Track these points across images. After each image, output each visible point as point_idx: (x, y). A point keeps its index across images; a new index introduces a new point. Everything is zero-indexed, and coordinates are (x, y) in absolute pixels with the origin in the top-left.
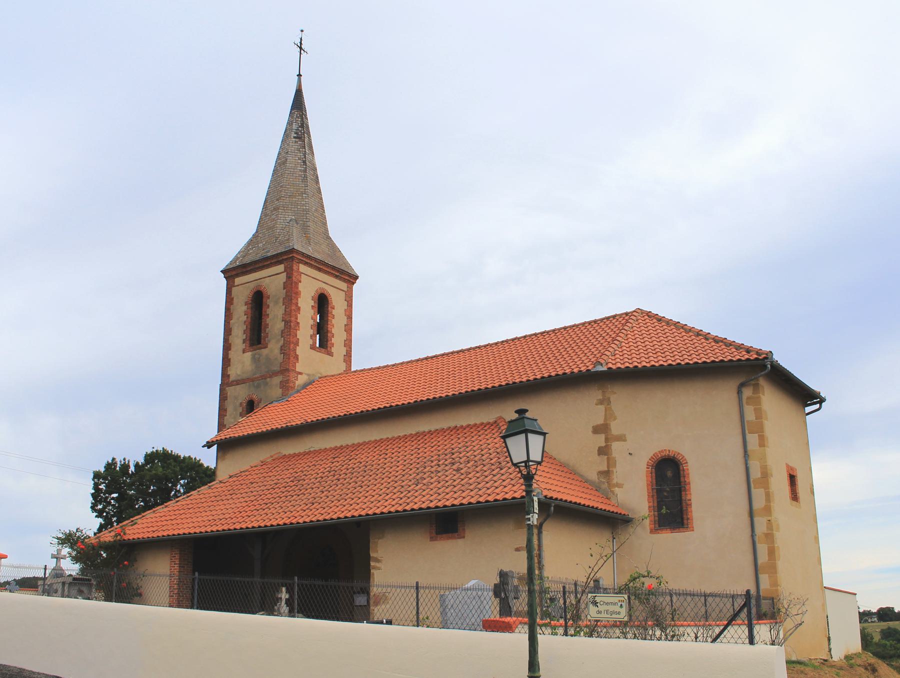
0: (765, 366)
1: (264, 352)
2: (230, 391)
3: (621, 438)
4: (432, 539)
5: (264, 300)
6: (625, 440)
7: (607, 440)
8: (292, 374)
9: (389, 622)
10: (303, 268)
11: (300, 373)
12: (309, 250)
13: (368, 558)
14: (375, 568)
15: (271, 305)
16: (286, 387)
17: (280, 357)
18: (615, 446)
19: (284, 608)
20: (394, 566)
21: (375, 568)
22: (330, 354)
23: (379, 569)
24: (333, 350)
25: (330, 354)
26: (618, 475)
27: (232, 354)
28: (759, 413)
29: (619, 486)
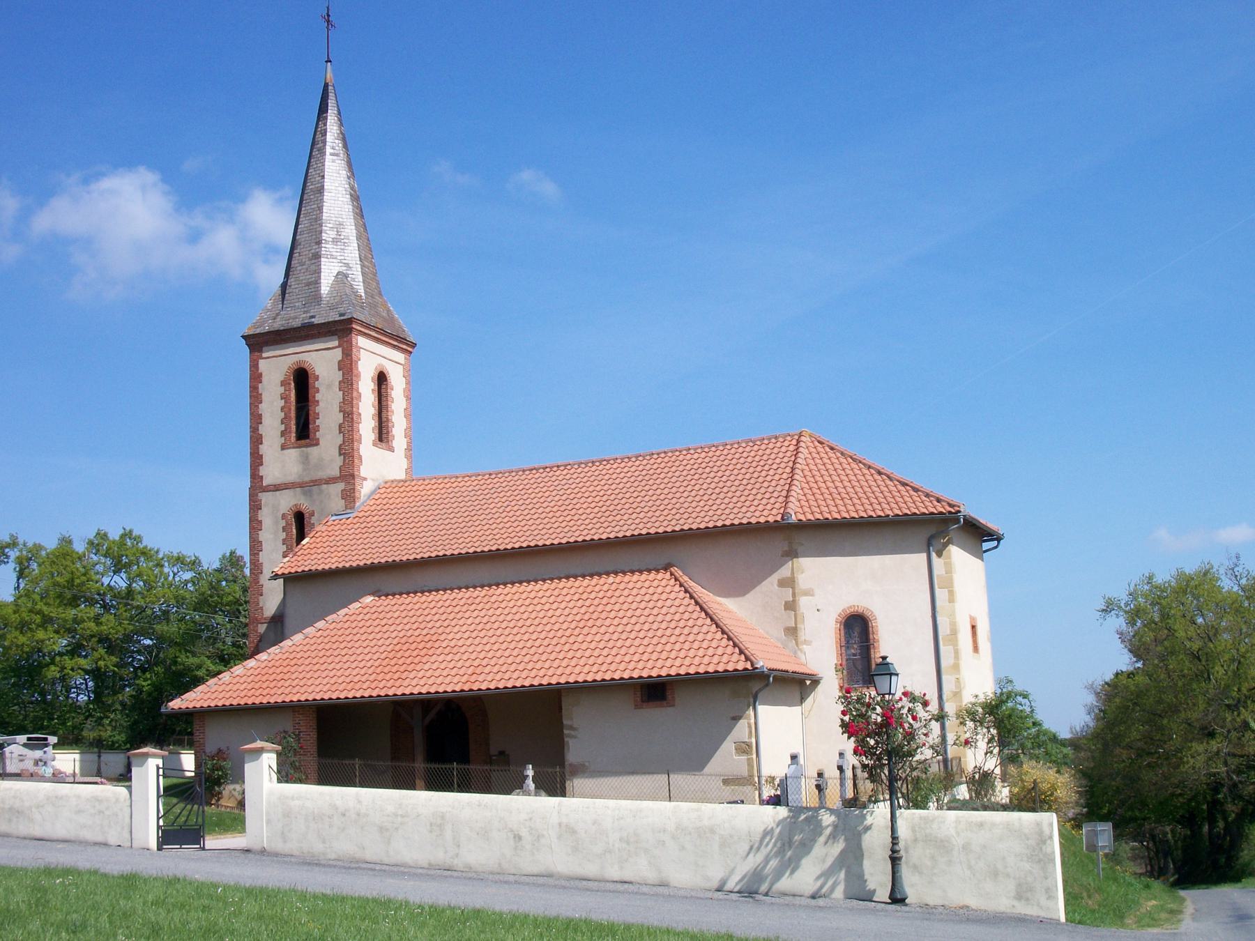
0: (957, 521)
1: (313, 451)
2: (265, 498)
3: (809, 593)
4: (637, 707)
5: (311, 381)
6: (813, 595)
7: (794, 595)
8: (358, 481)
9: (742, 802)
10: (362, 341)
11: (365, 479)
12: (361, 317)
13: (560, 726)
14: (569, 736)
15: (322, 389)
16: (349, 496)
17: (339, 461)
18: (803, 601)
19: (530, 784)
20: (584, 733)
21: (569, 736)
22: (391, 449)
23: (575, 737)
24: (395, 444)
25: (391, 449)
26: (806, 631)
27: (264, 449)
28: (949, 568)
29: (806, 642)
